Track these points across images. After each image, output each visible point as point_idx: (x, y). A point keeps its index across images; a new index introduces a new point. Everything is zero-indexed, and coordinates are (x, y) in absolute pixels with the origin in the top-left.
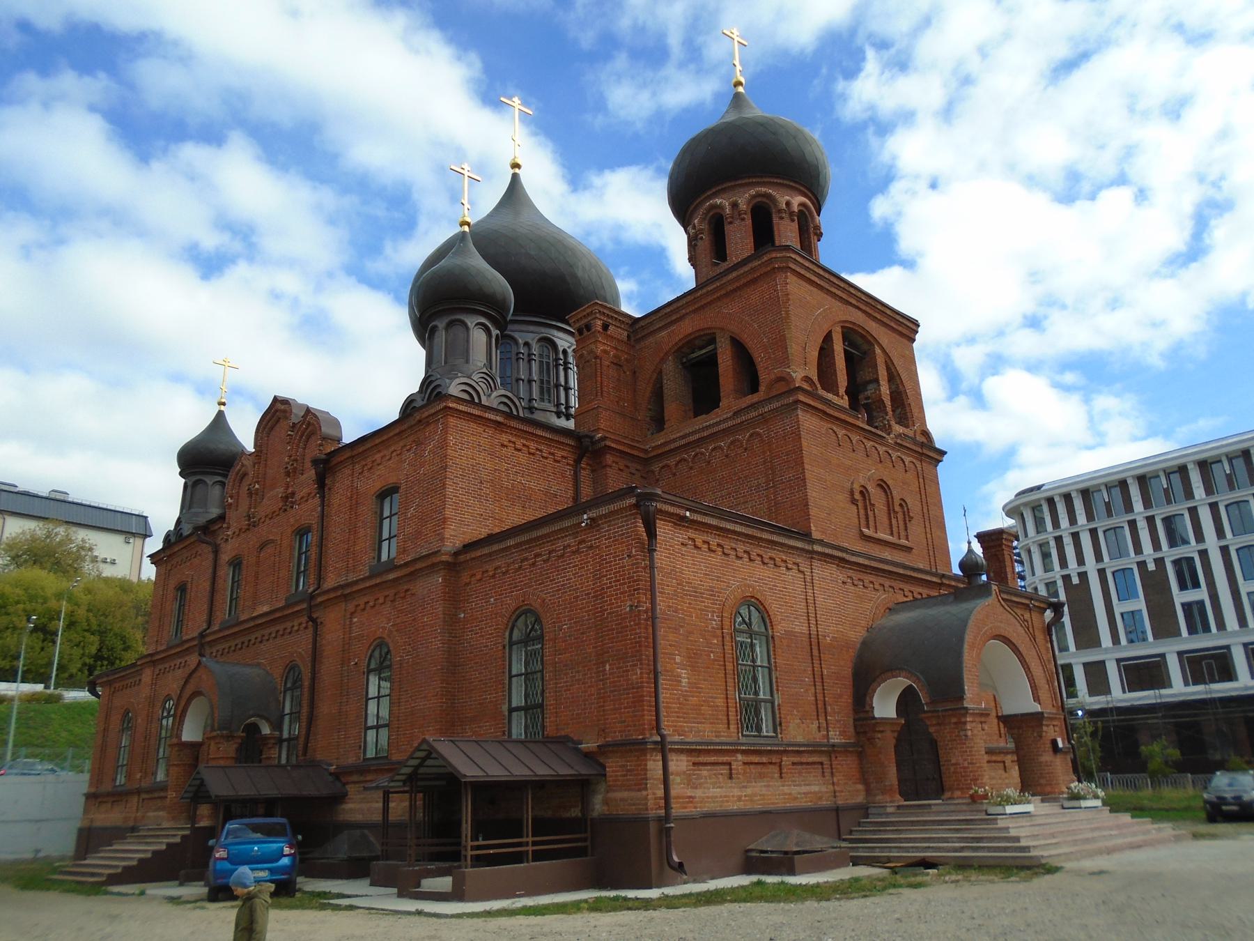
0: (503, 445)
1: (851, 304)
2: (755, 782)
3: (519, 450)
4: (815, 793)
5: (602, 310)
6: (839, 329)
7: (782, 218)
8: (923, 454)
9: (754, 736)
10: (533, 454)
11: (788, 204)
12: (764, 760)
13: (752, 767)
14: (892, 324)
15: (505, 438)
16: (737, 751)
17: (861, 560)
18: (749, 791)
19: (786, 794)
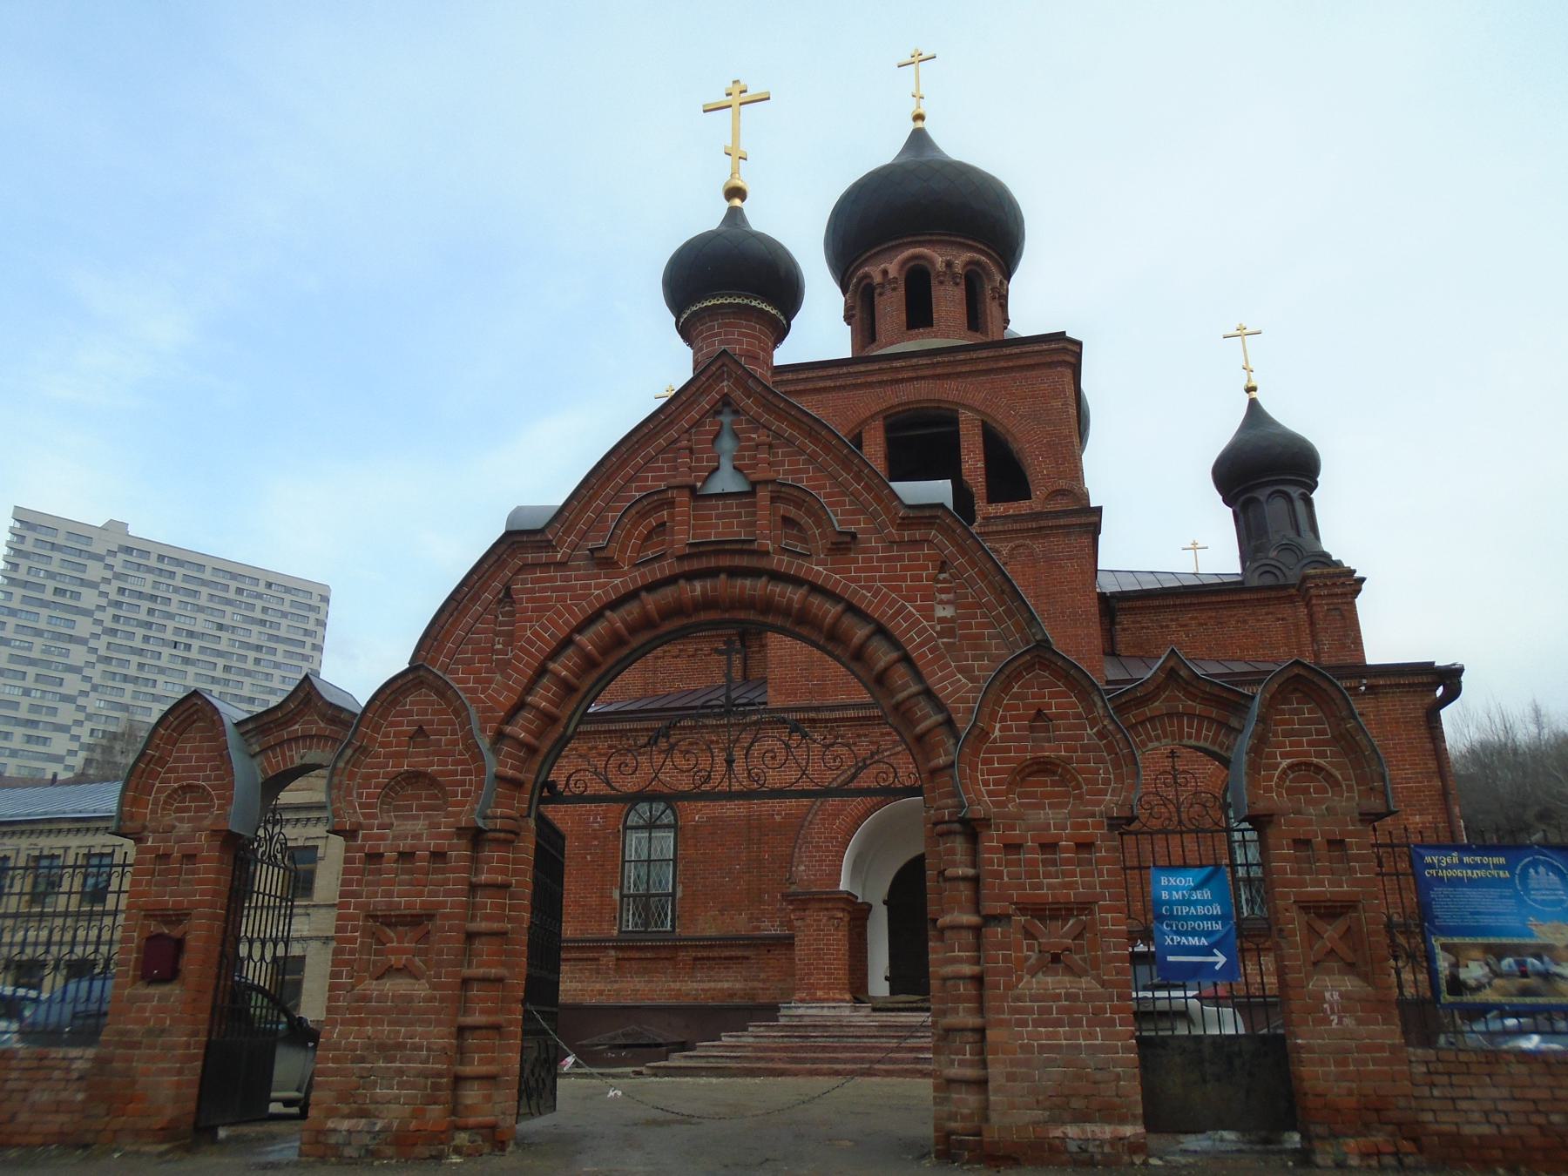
1: (902, 381)
2: (632, 977)
3: (676, 657)
4: (721, 990)
6: (878, 423)
7: (881, 294)
8: (1041, 528)
9: (641, 932)
10: (693, 656)
11: (885, 272)
12: (649, 955)
13: (633, 962)
14: (1002, 364)
16: (606, 948)
17: (851, 713)
18: (616, 986)
19: (674, 990)
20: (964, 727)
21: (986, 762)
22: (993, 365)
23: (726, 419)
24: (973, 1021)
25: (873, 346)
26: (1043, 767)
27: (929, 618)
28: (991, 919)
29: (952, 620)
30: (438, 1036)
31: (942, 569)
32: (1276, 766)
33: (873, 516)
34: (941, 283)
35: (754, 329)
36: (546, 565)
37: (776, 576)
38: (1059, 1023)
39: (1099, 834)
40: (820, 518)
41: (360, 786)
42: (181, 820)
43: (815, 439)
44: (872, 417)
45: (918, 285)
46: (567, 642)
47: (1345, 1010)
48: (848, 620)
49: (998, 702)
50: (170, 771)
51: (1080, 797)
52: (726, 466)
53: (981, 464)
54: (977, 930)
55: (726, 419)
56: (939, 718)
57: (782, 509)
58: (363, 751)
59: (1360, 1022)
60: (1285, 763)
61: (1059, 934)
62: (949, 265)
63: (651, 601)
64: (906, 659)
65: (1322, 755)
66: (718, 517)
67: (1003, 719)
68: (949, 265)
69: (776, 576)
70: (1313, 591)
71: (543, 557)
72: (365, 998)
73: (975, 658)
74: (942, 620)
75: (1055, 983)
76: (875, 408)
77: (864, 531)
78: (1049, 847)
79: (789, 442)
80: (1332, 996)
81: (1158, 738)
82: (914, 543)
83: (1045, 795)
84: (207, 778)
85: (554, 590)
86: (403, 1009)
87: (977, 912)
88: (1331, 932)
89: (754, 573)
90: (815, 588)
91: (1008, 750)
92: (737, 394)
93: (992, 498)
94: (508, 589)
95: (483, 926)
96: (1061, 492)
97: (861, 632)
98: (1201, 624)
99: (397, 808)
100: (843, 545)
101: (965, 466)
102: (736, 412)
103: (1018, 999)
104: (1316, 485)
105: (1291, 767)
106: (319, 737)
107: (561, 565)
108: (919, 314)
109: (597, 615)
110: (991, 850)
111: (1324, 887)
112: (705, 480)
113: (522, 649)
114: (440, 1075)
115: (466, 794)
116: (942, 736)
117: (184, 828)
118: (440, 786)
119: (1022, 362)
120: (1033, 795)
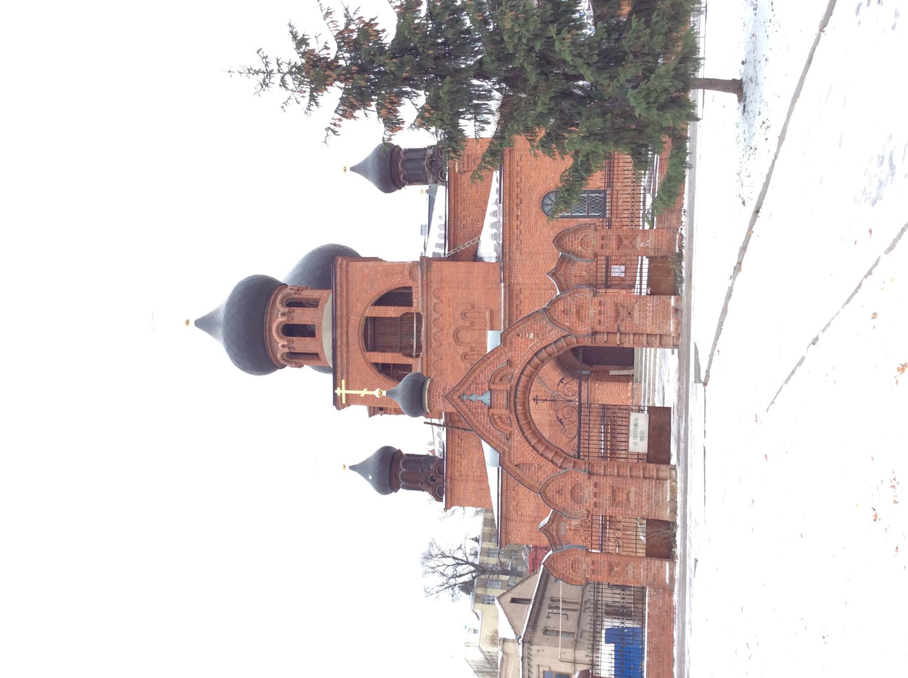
0: (461, 475)
1: (347, 342)
5: (372, 412)
6: (367, 354)
7: (294, 349)
11: (283, 346)
14: (345, 294)
15: (457, 474)
20: (565, 333)
21: (576, 327)
22: (345, 298)
23: (465, 398)
24: (645, 337)
25: (320, 355)
26: (578, 312)
27: (534, 340)
28: (619, 330)
29: (534, 334)
30: (646, 483)
31: (519, 335)
32: (581, 250)
33: (501, 354)
34: (292, 319)
35: (434, 388)
36: (509, 453)
37: (517, 384)
38: (646, 314)
39: (596, 300)
40: (500, 371)
41: (574, 510)
42: (582, 568)
43: (476, 370)
44: (364, 357)
45: (290, 330)
46: (533, 447)
47: (645, 242)
48: (532, 363)
49: (559, 323)
50: (566, 572)
51: (587, 303)
52: (480, 398)
53: (393, 308)
54: (621, 334)
55: (465, 398)
56: (562, 339)
57: (497, 380)
58: (564, 509)
59: (648, 239)
60: (580, 248)
61: (623, 313)
62: (283, 314)
63: (522, 422)
64: (545, 348)
65: (578, 238)
66: (497, 401)
67: (564, 322)
68: (283, 314)
69: (517, 384)
70: (465, 169)
71: (507, 454)
72: (635, 506)
73: (546, 327)
74: (534, 337)
75: (636, 315)
76: (360, 356)
77: (506, 357)
78: (600, 313)
79: (475, 378)
80: (642, 245)
81: (571, 280)
82: (511, 343)
83: (585, 312)
84: (569, 560)
85: (517, 451)
86: (639, 494)
87: (616, 333)
88: (625, 242)
89: (516, 389)
90: (522, 373)
91: (573, 322)
92: (458, 394)
93: (410, 304)
94: (517, 466)
95: (616, 471)
96: (410, 272)
97: (536, 360)
98: (464, 210)
99: (581, 499)
100: (510, 363)
101: (393, 315)
102: (463, 394)
103: (640, 324)
104: (397, 146)
105: (581, 246)
106: (557, 526)
107: (510, 448)
108: (307, 331)
109: (525, 437)
110: (600, 327)
111: (613, 243)
112: (485, 405)
113: (535, 461)
114: (656, 483)
115: (578, 477)
116: (567, 339)
117: (584, 566)
118: (575, 485)
119: (344, 285)
120: (585, 316)
